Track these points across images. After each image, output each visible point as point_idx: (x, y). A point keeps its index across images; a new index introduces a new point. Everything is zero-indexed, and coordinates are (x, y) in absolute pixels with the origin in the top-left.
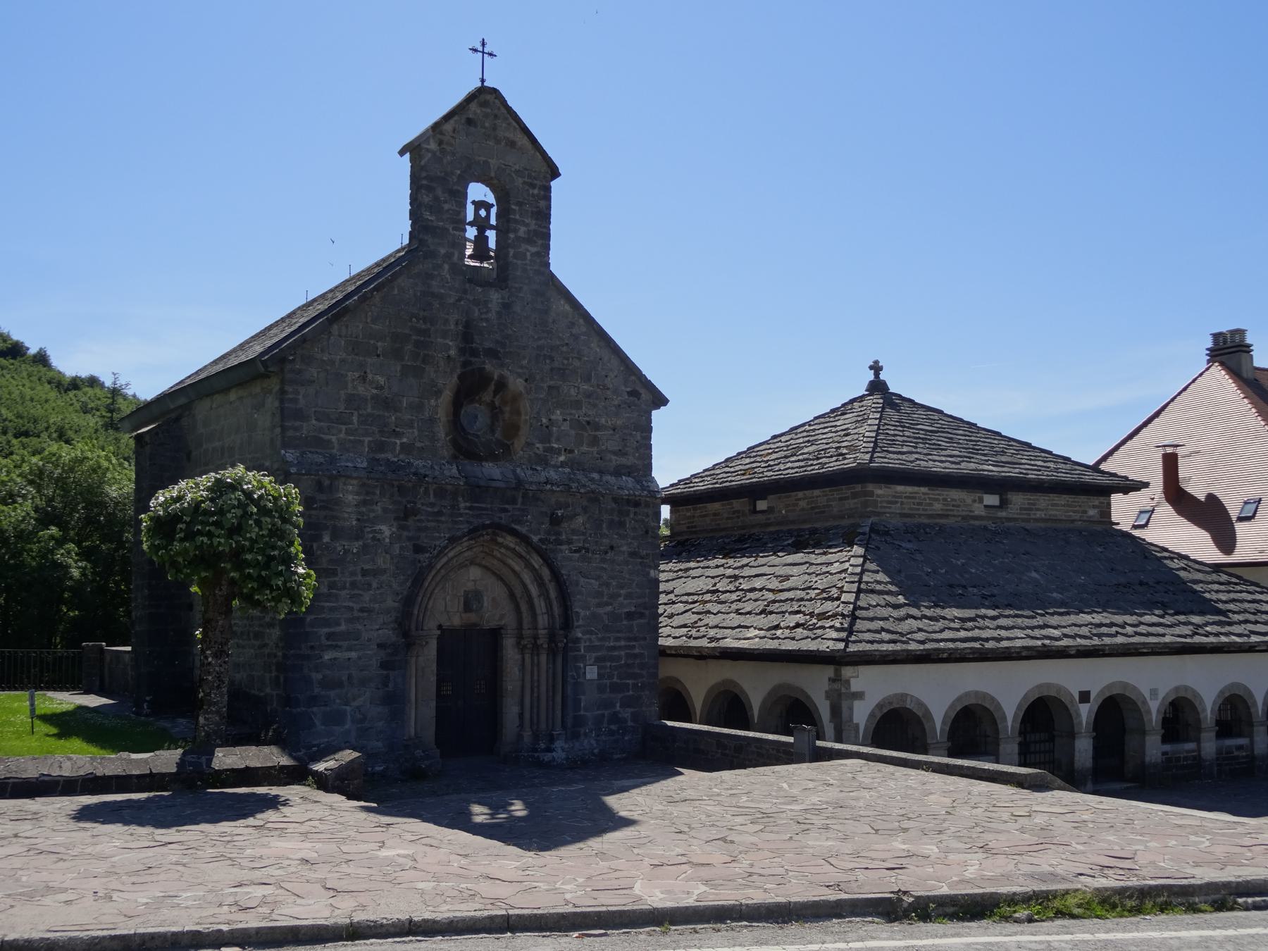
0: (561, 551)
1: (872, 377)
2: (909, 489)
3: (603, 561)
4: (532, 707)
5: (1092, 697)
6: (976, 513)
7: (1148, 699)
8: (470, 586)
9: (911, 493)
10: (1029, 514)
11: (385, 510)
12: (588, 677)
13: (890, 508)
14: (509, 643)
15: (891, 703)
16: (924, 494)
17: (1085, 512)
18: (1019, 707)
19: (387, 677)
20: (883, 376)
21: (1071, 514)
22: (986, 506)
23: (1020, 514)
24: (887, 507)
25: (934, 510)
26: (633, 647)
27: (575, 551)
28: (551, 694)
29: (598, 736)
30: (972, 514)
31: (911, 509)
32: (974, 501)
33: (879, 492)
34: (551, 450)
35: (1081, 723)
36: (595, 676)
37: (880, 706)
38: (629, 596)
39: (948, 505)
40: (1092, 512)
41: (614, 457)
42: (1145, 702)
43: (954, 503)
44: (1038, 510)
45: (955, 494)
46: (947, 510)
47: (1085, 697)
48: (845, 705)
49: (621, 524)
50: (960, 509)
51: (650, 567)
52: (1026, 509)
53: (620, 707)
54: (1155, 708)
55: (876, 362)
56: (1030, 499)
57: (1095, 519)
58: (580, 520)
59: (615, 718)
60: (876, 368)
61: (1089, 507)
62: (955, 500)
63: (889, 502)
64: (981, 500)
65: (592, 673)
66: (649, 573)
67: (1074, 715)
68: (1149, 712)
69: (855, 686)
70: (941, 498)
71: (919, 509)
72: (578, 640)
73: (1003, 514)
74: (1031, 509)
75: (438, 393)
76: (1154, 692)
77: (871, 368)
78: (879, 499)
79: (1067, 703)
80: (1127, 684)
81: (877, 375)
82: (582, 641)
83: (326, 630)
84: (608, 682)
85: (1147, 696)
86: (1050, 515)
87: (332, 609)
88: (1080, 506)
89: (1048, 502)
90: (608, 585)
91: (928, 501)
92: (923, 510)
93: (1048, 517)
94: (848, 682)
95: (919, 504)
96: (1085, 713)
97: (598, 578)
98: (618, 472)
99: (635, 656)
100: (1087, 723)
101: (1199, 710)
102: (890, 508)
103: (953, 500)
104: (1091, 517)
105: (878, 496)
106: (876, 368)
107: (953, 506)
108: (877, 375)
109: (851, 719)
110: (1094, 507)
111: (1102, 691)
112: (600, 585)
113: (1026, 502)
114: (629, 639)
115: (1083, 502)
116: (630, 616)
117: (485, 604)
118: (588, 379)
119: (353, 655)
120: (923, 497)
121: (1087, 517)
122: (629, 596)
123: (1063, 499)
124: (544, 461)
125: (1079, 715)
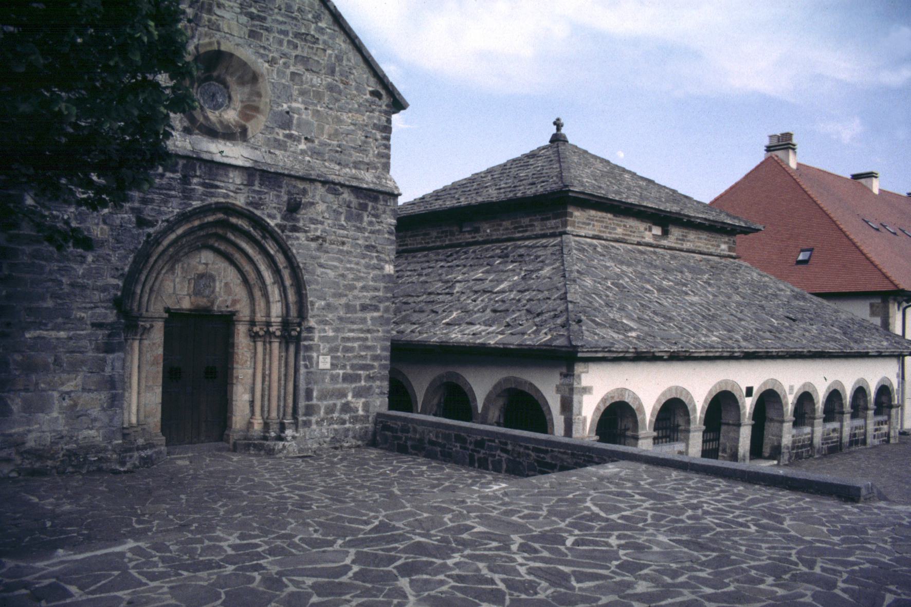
0: (298, 238)
1: (554, 131)
2: (600, 214)
4: (263, 396)
8: (201, 268)
12: (321, 366)
14: (241, 330)
15: (612, 397)
16: (609, 219)
19: (104, 360)
20: (563, 131)
22: (653, 235)
25: (617, 234)
26: (366, 339)
27: (313, 240)
28: (283, 382)
29: (330, 424)
31: (600, 231)
32: (646, 229)
34: (290, 136)
35: (745, 413)
36: (328, 366)
37: (604, 400)
38: (364, 288)
42: (785, 396)
43: (631, 229)
44: (688, 241)
46: (626, 235)
48: (576, 398)
49: (359, 218)
50: (636, 235)
53: (353, 397)
54: (790, 400)
55: (558, 119)
59: (346, 408)
60: (558, 124)
64: (650, 230)
65: (325, 363)
66: (382, 268)
67: (741, 408)
70: (622, 224)
72: (310, 329)
73: (664, 242)
76: (791, 388)
77: (555, 123)
81: (558, 129)
82: (316, 331)
84: (341, 372)
85: (787, 392)
90: (343, 276)
94: (579, 376)
96: (748, 404)
98: (356, 165)
99: (368, 348)
100: (750, 413)
103: (630, 226)
106: (558, 124)
107: (631, 231)
108: (558, 129)
109: (580, 414)
110: (725, 243)
111: (760, 387)
114: (362, 331)
116: (364, 308)
117: (217, 289)
118: (332, 72)
122: (364, 288)
124: (281, 145)
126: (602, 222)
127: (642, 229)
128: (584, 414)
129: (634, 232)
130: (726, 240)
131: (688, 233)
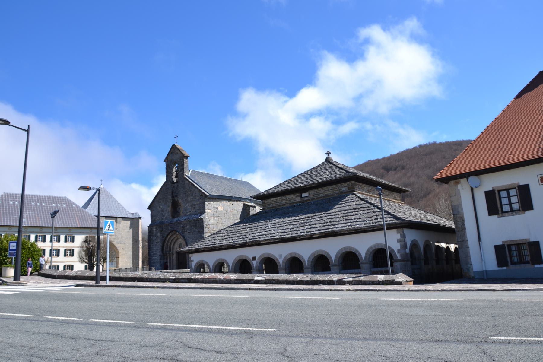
1: (327, 156)
2: (275, 199)
3: (193, 234)
5: (257, 258)
6: (297, 201)
7: (278, 258)
8: (180, 243)
9: (275, 200)
10: (317, 196)
11: (159, 231)
13: (270, 206)
15: (199, 263)
16: (279, 199)
17: (341, 189)
18: (233, 262)
21: (334, 192)
23: (313, 197)
24: (268, 206)
27: (188, 233)
30: (296, 201)
31: (276, 205)
32: (296, 197)
33: (266, 202)
35: (254, 267)
37: (197, 263)
39: (287, 200)
40: (344, 189)
41: (198, 211)
42: (277, 259)
45: (290, 196)
47: (254, 258)
49: (196, 226)
51: (202, 234)
52: (315, 195)
56: (317, 191)
57: (346, 191)
58: (188, 226)
61: (343, 187)
62: (290, 198)
63: (269, 204)
68: (279, 263)
69: (192, 259)
70: (285, 199)
71: (278, 204)
74: (318, 194)
75: (169, 207)
76: (280, 256)
77: (326, 154)
78: (266, 204)
79: (249, 261)
80: (270, 254)
81: (328, 155)
83: (152, 253)
85: (278, 257)
86: (326, 195)
87: (153, 250)
88: (339, 188)
89: (324, 190)
90: (194, 239)
91: (281, 201)
92: (280, 204)
93: (325, 195)
94: (190, 258)
95: (278, 203)
97: (192, 238)
101: (302, 261)
102: (270, 206)
103: (289, 198)
104: (344, 191)
105: (266, 203)
107: (289, 200)
109: (191, 267)
110: (345, 187)
111: (260, 256)
112: (192, 240)
113: (315, 192)
115: (340, 186)
118: (192, 195)
119: (156, 257)
120: (279, 200)
121: (342, 191)
123: (331, 187)
125: (253, 264)
126: (277, 201)
127: (295, 197)
128: (192, 267)
129: (291, 200)
130: (346, 185)
131: (320, 190)
